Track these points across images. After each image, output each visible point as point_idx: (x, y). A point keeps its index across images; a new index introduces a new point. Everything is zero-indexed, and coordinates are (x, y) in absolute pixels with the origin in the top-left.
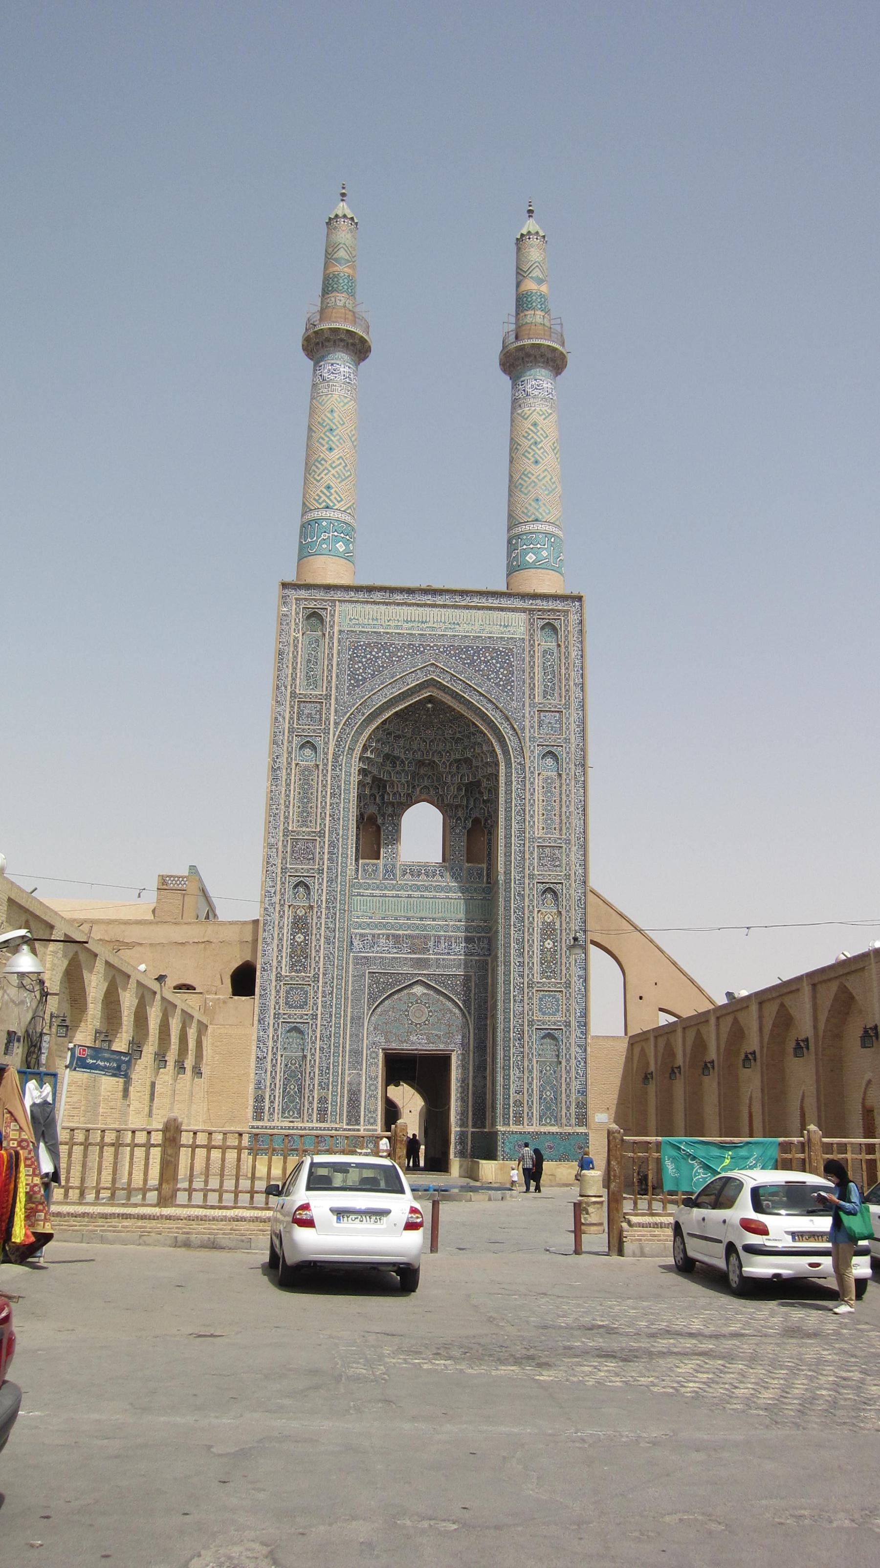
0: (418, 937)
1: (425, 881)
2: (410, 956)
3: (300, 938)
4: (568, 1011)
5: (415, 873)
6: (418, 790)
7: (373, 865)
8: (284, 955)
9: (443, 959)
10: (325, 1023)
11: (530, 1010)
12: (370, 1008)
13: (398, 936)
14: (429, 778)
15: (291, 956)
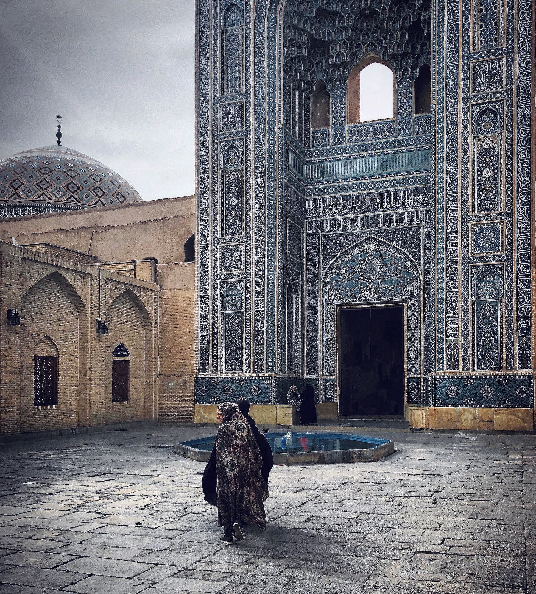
0: (368, 195)
1: (373, 139)
2: (360, 215)
3: (234, 201)
4: (509, 243)
5: (364, 133)
6: (364, 48)
7: (323, 131)
8: (219, 219)
9: (393, 214)
10: (259, 280)
11: (465, 247)
12: (324, 269)
13: (349, 197)
14: (373, 33)
15: (227, 220)
